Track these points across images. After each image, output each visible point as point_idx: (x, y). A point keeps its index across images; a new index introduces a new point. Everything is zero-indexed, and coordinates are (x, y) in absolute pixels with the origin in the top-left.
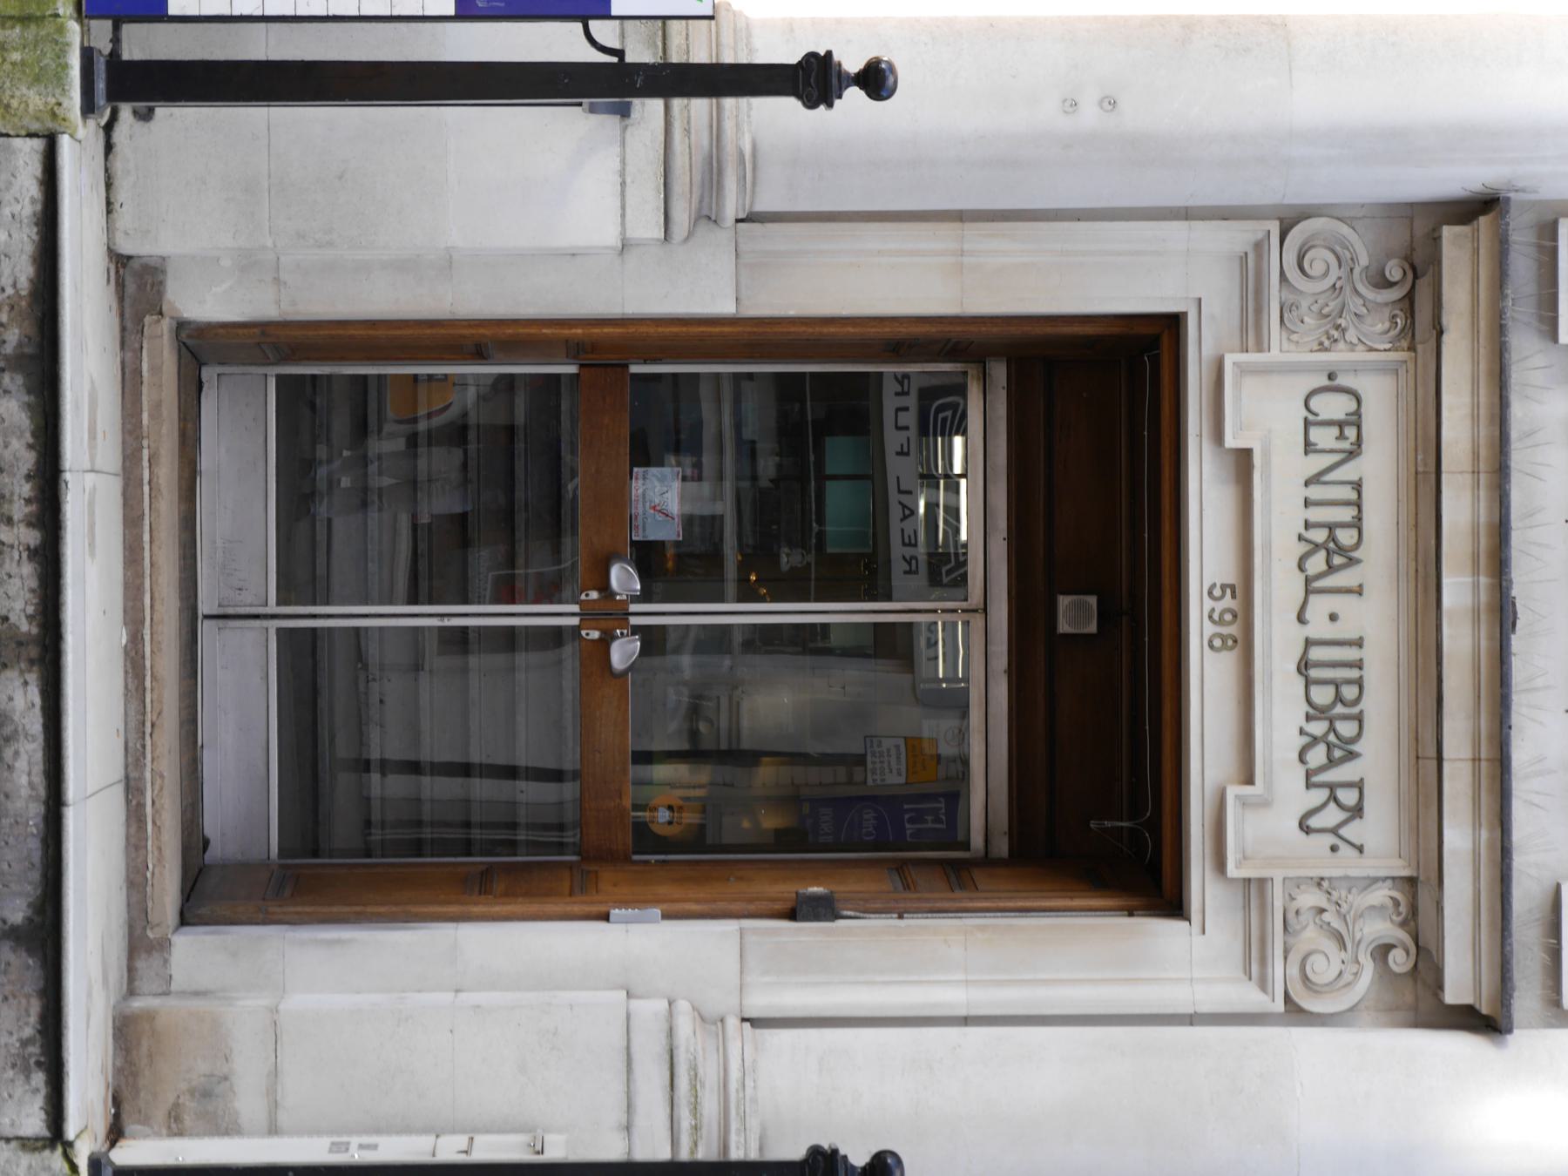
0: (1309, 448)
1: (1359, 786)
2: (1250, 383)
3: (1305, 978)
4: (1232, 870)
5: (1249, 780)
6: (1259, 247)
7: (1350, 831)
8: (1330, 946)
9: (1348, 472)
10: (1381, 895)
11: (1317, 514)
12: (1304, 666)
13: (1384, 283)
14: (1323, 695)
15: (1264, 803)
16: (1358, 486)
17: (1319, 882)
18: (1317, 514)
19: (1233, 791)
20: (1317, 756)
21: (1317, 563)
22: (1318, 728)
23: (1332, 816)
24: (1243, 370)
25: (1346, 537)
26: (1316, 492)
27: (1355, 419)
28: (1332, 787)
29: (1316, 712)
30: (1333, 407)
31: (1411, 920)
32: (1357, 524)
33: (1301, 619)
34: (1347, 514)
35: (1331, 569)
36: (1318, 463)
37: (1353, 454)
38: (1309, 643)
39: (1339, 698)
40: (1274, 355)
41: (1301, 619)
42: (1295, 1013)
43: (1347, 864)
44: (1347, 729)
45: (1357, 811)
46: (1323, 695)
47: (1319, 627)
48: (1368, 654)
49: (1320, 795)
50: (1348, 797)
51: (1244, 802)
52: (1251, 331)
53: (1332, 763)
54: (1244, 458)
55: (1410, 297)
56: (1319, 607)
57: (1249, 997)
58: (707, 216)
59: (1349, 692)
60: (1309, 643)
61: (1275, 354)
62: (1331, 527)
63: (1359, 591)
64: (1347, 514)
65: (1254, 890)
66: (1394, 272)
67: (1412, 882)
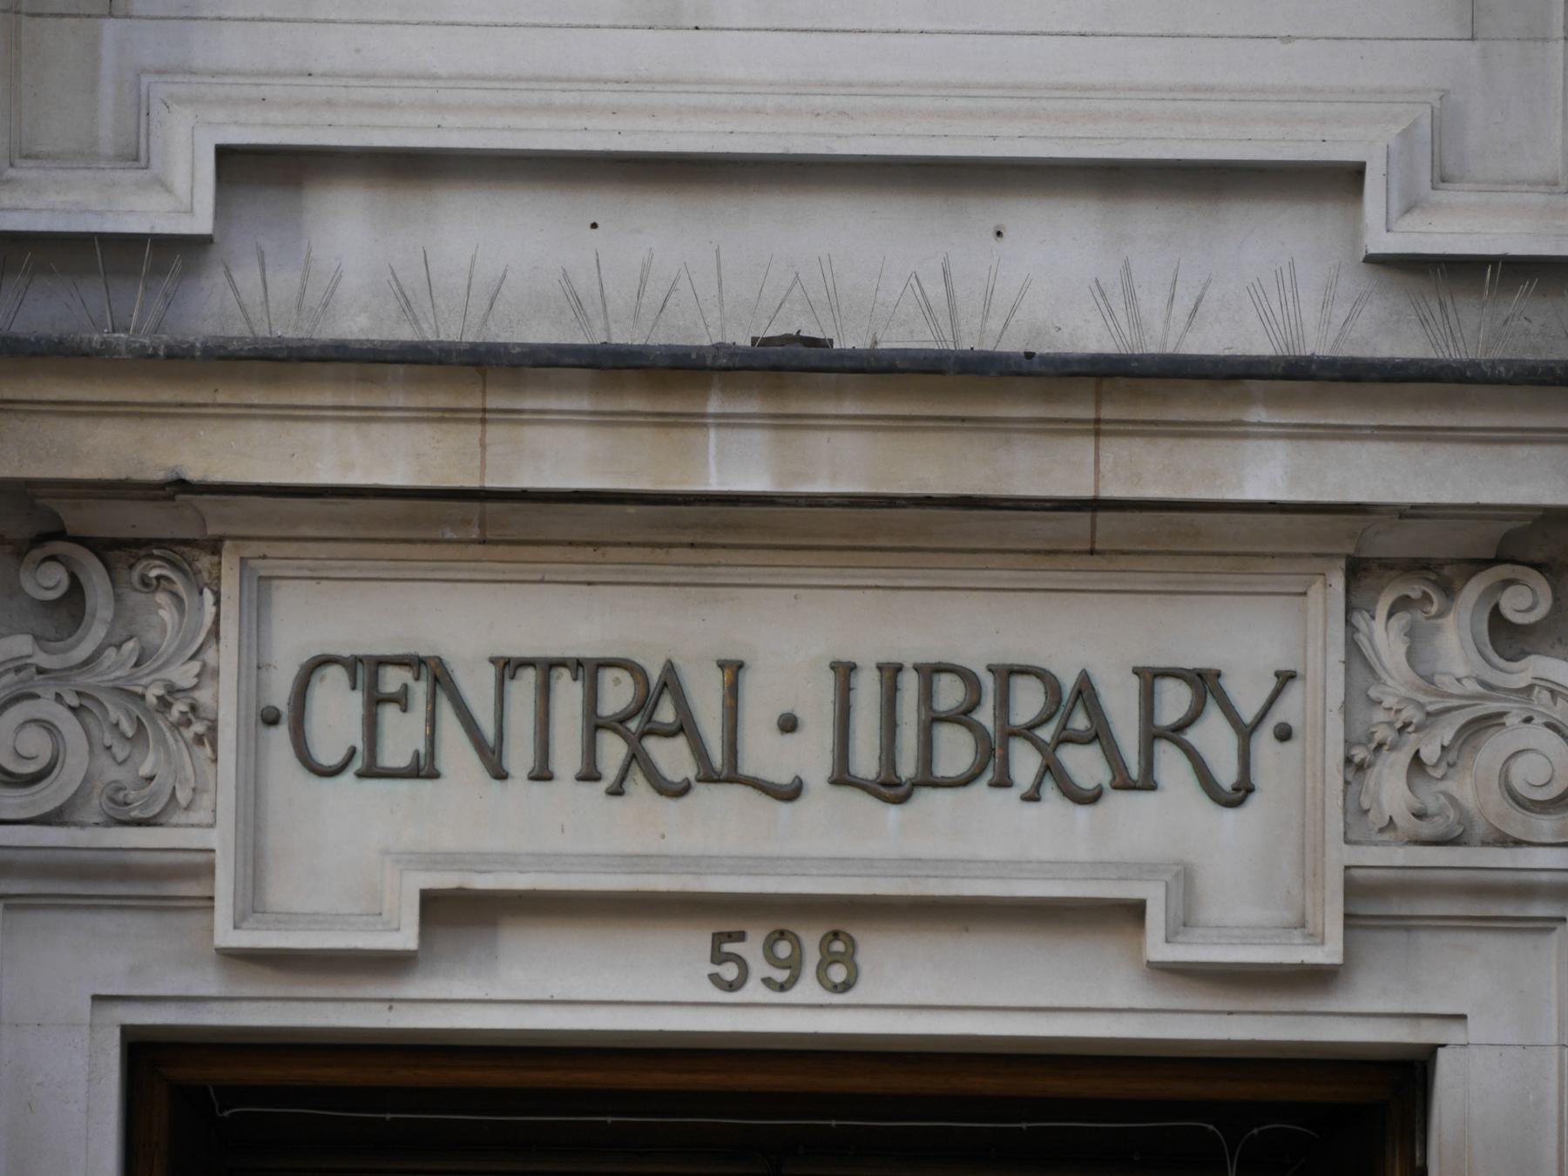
0: (423, 769)
1: (1149, 678)
2: (281, 893)
4: (1328, 953)
5: (1135, 911)
8: (1493, 748)
9: (477, 688)
11: (568, 755)
12: (891, 790)
13: (73, 602)
14: (955, 748)
15: (1184, 881)
16: (507, 667)
17: (1355, 768)
19: (1158, 948)
20: (1085, 765)
21: (672, 757)
22: (1025, 763)
24: (251, 907)
25: (617, 694)
26: (520, 756)
28: (1151, 735)
32: (588, 670)
33: (791, 793)
34: (568, 694)
35: (685, 727)
37: (438, 675)
38: (842, 777)
39: (962, 717)
40: (220, 840)
41: (791, 793)
44: (1028, 701)
45: (1205, 683)
46: (955, 748)
48: (868, 651)
49: (1169, 760)
50: (1174, 701)
51: (1183, 924)
53: (1100, 734)
55: (109, 549)
59: (950, 693)
60: (842, 777)
61: (220, 840)
62: (595, 725)
63: (733, 670)
64: (568, 694)
66: (49, 581)
67: (1359, 571)
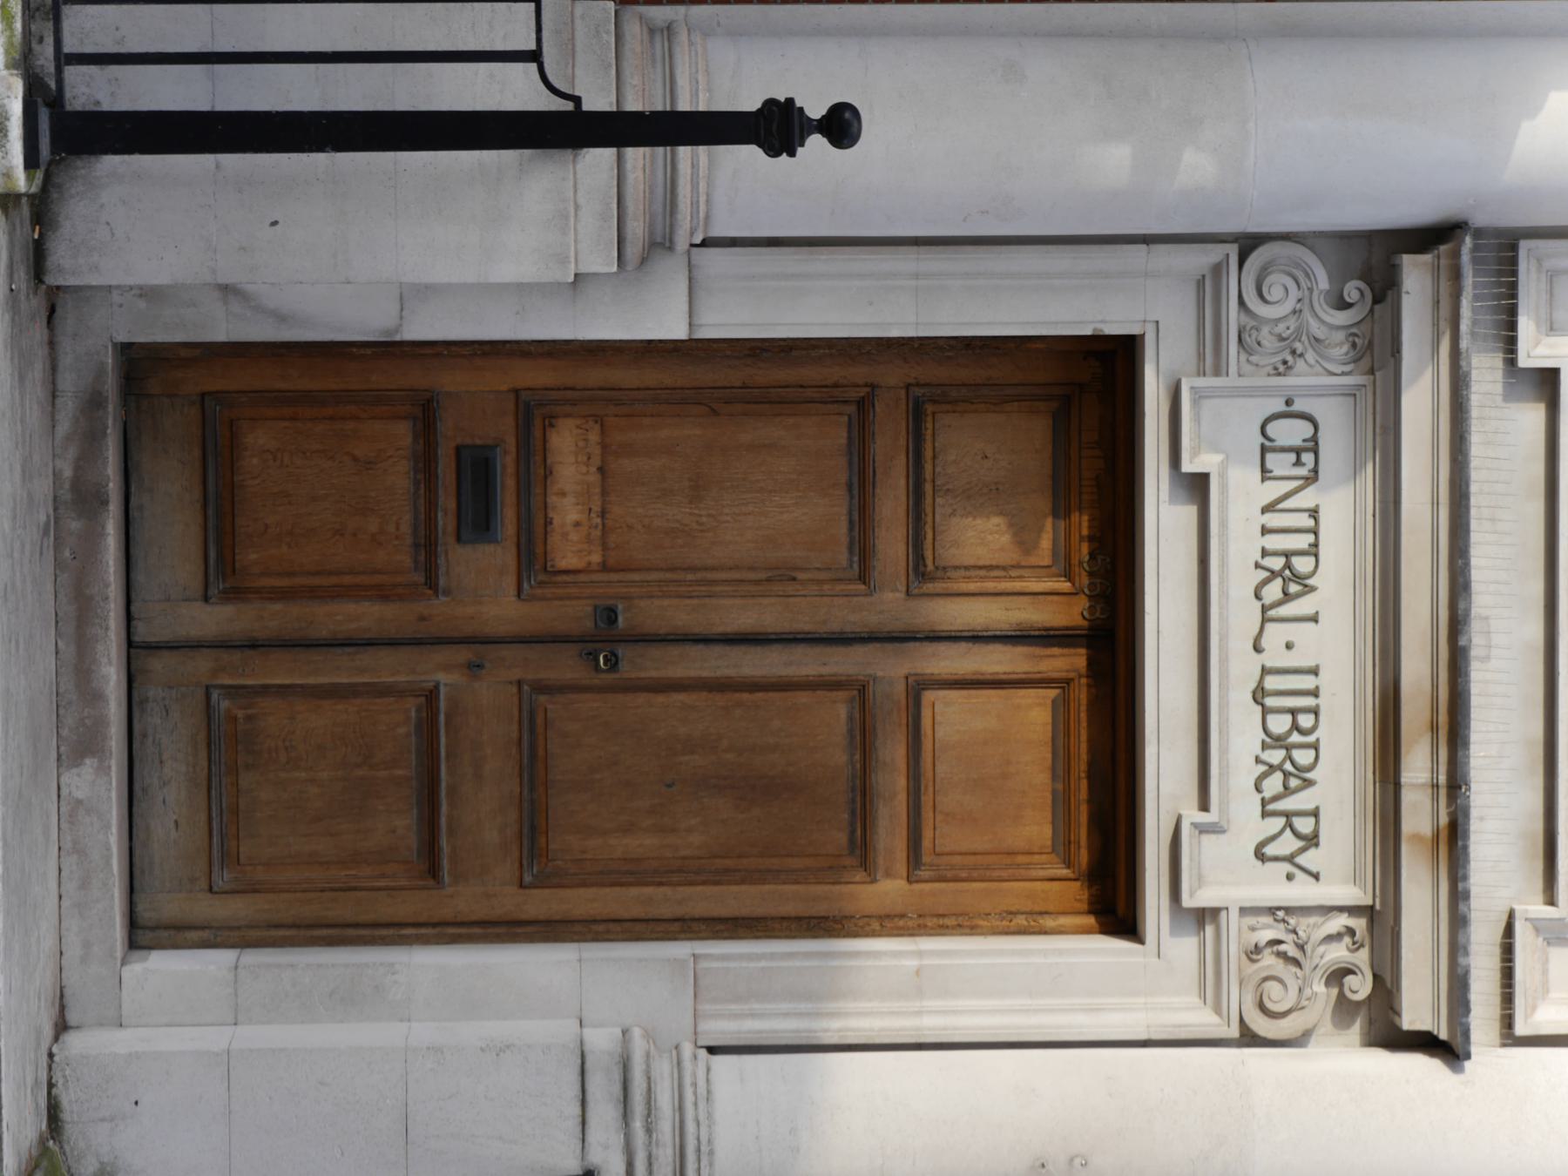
1: (1315, 813)
3: (1262, 1007)
5: (1204, 806)
6: (1218, 270)
7: (1309, 859)
9: (1306, 499)
11: (1276, 542)
12: (1259, 694)
14: (1280, 724)
16: (1314, 513)
18: (1276, 542)
20: (1274, 784)
21: (1273, 591)
22: (1276, 756)
23: (1288, 844)
25: (1302, 565)
26: (1274, 520)
27: (1313, 445)
28: (1288, 815)
29: (1276, 741)
30: (1291, 432)
32: (1313, 551)
33: (1257, 648)
34: (1303, 541)
35: (1287, 597)
36: (1275, 490)
38: (1265, 671)
39: (1295, 727)
41: (1257, 648)
42: (1249, 1038)
43: (1302, 892)
44: (1303, 757)
45: (1312, 840)
47: (1275, 656)
48: (1323, 681)
50: (1304, 825)
51: (1203, 829)
53: (1287, 791)
56: (1275, 635)
57: (1204, 1020)
59: (1305, 721)
60: (1265, 671)
62: (1287, 555)
63: (1314, 619)
64: (1303, 541)
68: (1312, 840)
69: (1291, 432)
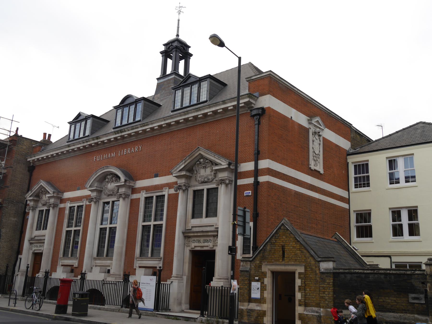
4: (212, 247)
6: (186, 246)
10: (214, 238)
14: (205, 242)
15: (210, 245)
23: (211, 241)
24: (191, 247)
30: (193, 241)
31: (215, 236)
37: (195, 240)
47: (202, 242)
51: (210, 246)
52: (189, 246)
54: (195, 246)
56: (201, 242)
58: (181, 277)
61: (190, 245)
65: (213, 246)
68: (210, 240)
69: (193, 241)
